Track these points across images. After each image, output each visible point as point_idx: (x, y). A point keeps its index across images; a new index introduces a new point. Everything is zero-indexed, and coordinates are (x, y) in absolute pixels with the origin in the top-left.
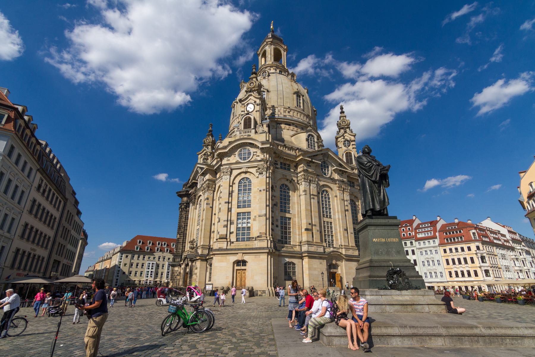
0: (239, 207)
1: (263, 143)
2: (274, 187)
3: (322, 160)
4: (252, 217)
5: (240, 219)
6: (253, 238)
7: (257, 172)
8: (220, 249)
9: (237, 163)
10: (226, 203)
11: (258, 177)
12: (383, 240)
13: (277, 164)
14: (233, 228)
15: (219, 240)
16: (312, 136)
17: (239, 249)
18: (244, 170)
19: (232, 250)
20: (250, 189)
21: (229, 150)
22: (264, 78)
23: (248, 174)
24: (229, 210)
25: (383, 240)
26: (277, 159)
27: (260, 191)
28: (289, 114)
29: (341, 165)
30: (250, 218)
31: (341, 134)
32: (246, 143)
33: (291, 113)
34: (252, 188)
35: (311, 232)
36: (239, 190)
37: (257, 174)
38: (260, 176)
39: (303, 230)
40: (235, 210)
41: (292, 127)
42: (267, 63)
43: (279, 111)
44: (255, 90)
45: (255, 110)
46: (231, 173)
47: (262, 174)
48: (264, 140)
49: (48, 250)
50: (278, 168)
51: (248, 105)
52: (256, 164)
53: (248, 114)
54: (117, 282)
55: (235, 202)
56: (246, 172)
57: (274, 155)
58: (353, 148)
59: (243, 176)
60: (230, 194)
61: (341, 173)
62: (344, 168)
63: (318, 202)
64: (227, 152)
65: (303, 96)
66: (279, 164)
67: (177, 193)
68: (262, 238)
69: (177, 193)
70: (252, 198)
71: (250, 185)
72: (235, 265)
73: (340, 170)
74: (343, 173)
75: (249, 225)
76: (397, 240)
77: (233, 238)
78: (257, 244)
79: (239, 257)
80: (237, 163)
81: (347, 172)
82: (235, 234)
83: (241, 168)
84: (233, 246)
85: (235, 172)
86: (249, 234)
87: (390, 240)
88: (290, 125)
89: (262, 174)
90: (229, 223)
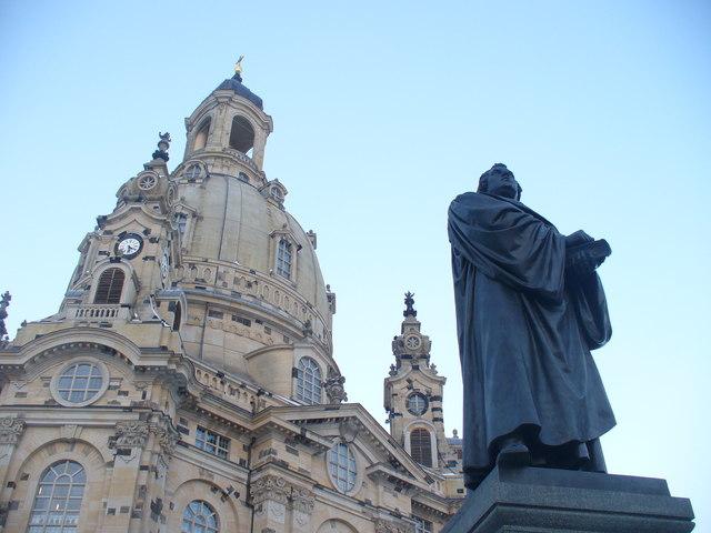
1: (146, 351)
2: (166, 506)
3: (336, 440)
7: (111, 446)
9: (51, 405)
11: (111, 464)
13: (186, 432)
16: (314, 363)
18: (68, 433)
21: (32, 361)
22: (192, 181)
23: (78, 448)
26: (186, 415)
27: (112, 511)
28: (250, 291)
29: (394, 463)
31: (402, 374)
32: (92, 345)
33: (258, 290)
34: (85, 499)
37: (109, 455)
38: (120, 461)
41: (255, 327)
42: (208, 148)
43: (219, 277)
44: (152, 200)
45: (142, 255)
46: (20, 437)
47: (128, 453)
48: (153, 342)
50: (186, 445)
51: (123, 236)
52: (111, 418)
53: (117, 260)
56: (73, 442)
57: (178, 399)
58: (435, 420)
59: (62, 453)
61: (393, 486)
62: (405, 471)
64: (21, 366)
65: (300, 247)
66: (192, 428)
73: (392, 479)
74: (398, 490)
80: (51, 405)
81: (409, 486)
83: (58, 426)
85: (37, 438)
88: (247, 323)
89: (128, 453)
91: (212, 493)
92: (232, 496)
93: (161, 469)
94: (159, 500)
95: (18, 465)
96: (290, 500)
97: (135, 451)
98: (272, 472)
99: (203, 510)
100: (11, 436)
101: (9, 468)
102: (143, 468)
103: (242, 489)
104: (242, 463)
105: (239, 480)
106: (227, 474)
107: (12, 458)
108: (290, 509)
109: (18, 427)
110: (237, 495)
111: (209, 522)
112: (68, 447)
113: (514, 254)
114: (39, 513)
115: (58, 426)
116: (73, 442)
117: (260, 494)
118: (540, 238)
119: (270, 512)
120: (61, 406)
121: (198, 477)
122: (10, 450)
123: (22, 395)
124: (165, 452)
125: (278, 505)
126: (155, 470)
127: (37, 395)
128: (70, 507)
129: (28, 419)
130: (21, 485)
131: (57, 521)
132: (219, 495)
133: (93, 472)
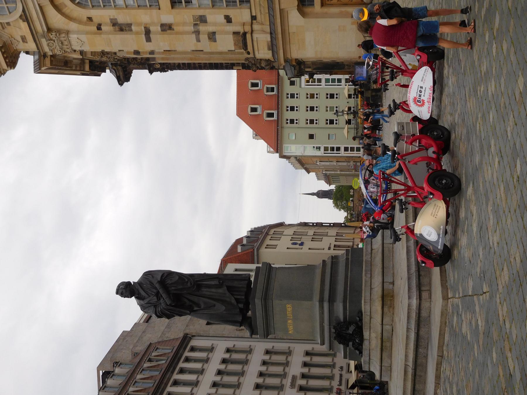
8: (272, 46)
9: (25, 17)
10: (148, 39)
14: (216, 17)
15: (250, 49)
19: (272, 24)
24: (166, 28)
25: (289, 321)
40: (168, 16)
46: (59, 32)
49: (292, 345)
54: (352, 149)
55: (145, 17)
60: (122, 28)
67: (121, 83)
69: (121, 83)
72: (308, 10)
77: (241, 15)
80: (25, 17)
82: (232, 12)
84: (263, 17)
85: (56, 20)
90: (202, 28)
95: (82, 27)
100: (62, 39)
101: (87, 33)
107: (78, 32)
109: (53, 36)
115: (41, 8)
120: (24, 11)
122: (73, 37)
123: (24, 39)
127: (20, 29)
129: (43, 31)
130: (96, 20)
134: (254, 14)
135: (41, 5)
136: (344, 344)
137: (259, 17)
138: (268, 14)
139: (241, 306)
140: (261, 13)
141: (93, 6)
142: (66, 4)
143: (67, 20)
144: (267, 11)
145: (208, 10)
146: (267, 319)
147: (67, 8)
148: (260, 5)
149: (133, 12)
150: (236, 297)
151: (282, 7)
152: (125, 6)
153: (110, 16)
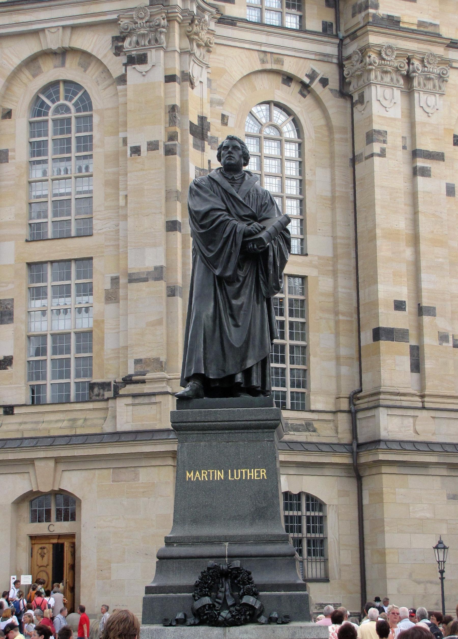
0: (36, 234)
2: (214, 122)
4: (101, 281)
5: (38, 293)
6: (105, 386)
7: (118, 51)
12: (220, 475)
17: (37, 442)
18: (53, 42)
20: (86, 143)
25: (220, 475)
27: (136, 150)
30: (86, 289)
34: (96, 134)
35: (405, 347)
36: (37, 149)
37: (116, 65)
38: (133, 74)
39: (367, 337)
50: (232, 22)
59: (50, 72)
63: (451, 191)
68: (146, 388)
70: (97, 188)
71: (86, 122)
75: (85, 323)
76: (263, 472)
78: (126, 415)
79: (42, 478)
82: (19, 369)
86: (86, 366)
87: (237, 475)
91: (285, 87)
92: (316, 86)
93: (195, 71)
94: (202, 119)
96: (408, 78)
97: (153, 56)
98: (373, 39)
99: (279, 117)
102: (170, 79)
103: (329, 71)
104: (326, 27)
105: (324, 58)
106: (305, 56)
108: (409, 92)
110: (324, 82)
111: (289, 132)
112: (58, 61)
113: (209, 247)
114: (39, 162)
115: (36, 33)
116: (63, 53)
117: (360, 76)
118: (225, 236)
119: (376, 109)
121: (259, 67)
124: (199, 46)
125: (388, 91)
126: (187, 78)
128: (79, 149)
131: (66, 171)
132: (295, 88)
133: (101, 97)
134: (16, 411)
135: (41, 35)
136: (196, 586)
137: (9, 419)
138: (19, 436)
139: (239, 378)
140: (21, 424)
141: (31, 123)
142: (38, 78)
143: (8, 73)
144: (26, 436)
145: (23, 327)
146: (223, 429)
147: (31, 77)
148: (37, 423)
149: (22, 194)
150: (255, 368)
151: (37, 463)
152: (30, 180)
153: (14, 150)
